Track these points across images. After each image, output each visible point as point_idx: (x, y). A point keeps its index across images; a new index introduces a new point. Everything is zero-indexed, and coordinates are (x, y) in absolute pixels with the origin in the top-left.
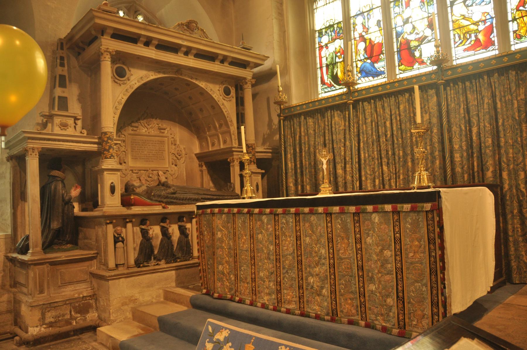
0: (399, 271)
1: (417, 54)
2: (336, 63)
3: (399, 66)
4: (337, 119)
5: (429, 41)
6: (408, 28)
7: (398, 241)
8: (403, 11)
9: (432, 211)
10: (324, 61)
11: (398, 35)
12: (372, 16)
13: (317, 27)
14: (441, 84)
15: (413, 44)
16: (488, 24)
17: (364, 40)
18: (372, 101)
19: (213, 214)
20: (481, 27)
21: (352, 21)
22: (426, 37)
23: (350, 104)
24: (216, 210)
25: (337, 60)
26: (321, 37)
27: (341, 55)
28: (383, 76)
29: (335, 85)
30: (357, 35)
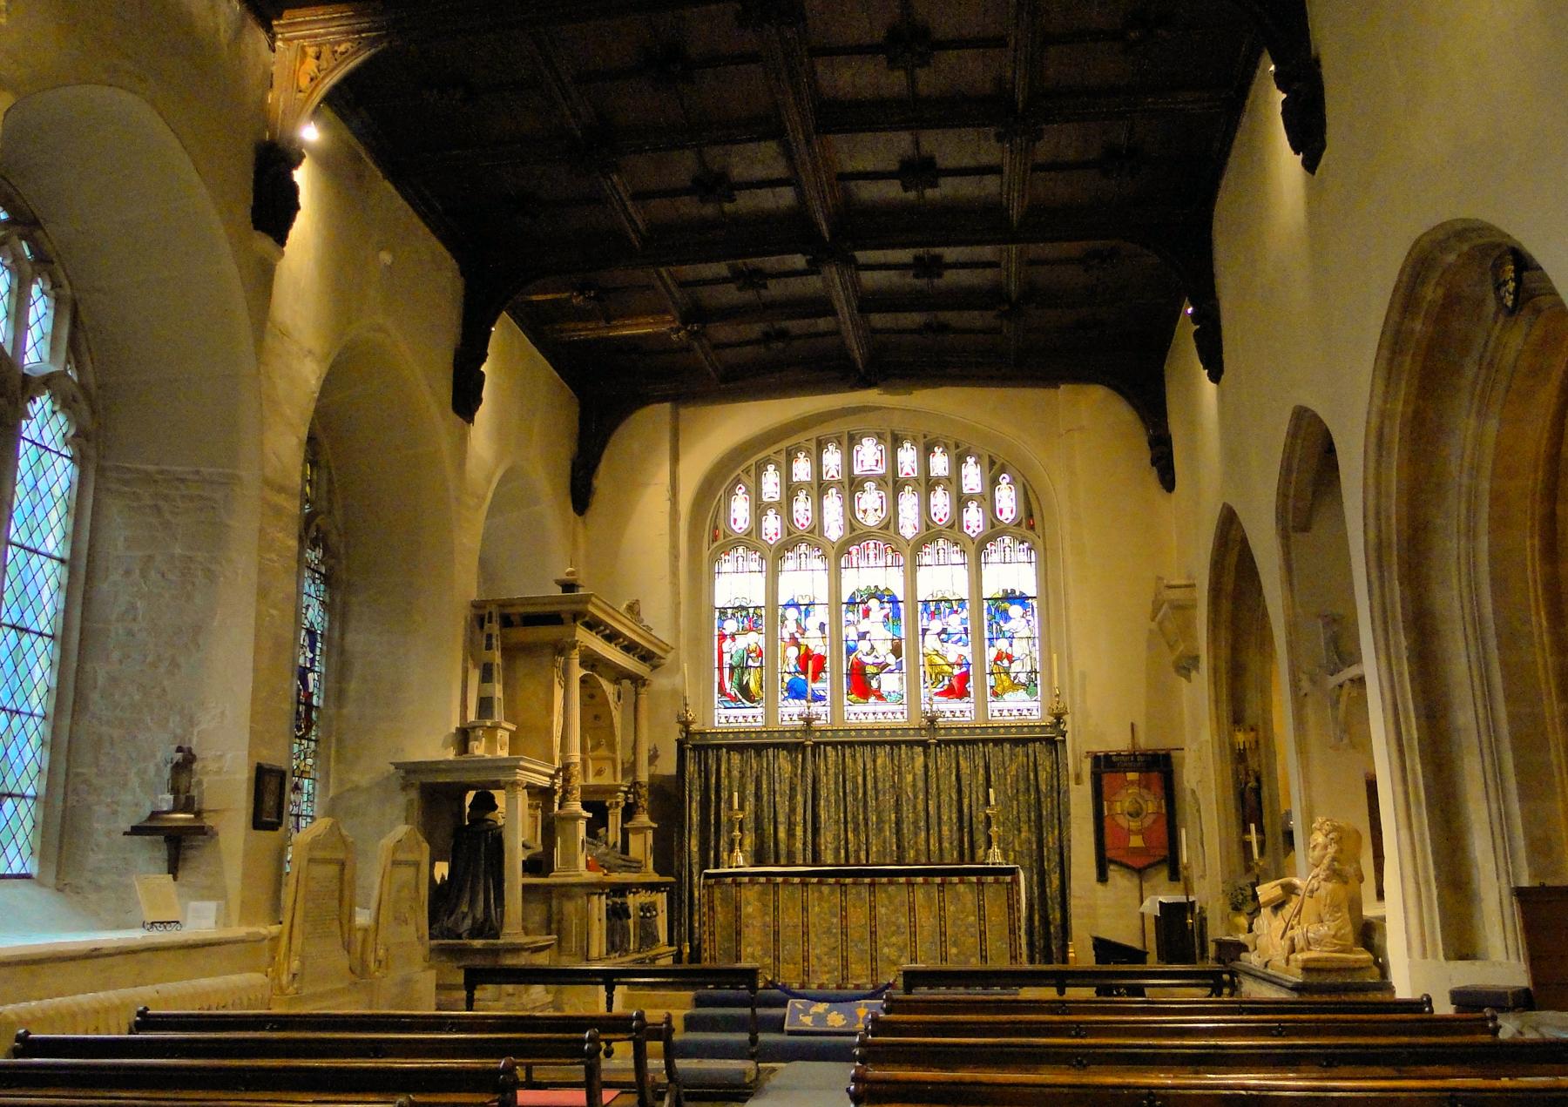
0: (982, 933)
1: (874, 684)
2: (748, 667)
3: (848, 694)
4: (783, 762)
5: (891, 672)
6: (864, 646)
7: (981, 908)
8: (858, 621)
9: (1011, 883)
10: (726, 658)
11: (851, 651)
12: (812, 614)
13: (719, 604)
14: (933, 744)
15: (870, 670)
16: (964, 669)
17: (798, 645)
18: (839, 747)
19: (739, 885)
20: (957, 671)
21: (780, 612)
22: (888, 665)
23: (808, 746)
24: (746, 879)
25: (750, 662)
26: (724, 620)
27: (758, 656)
28: (823, 703)
29: (743, 700)
30: (787, 636)
